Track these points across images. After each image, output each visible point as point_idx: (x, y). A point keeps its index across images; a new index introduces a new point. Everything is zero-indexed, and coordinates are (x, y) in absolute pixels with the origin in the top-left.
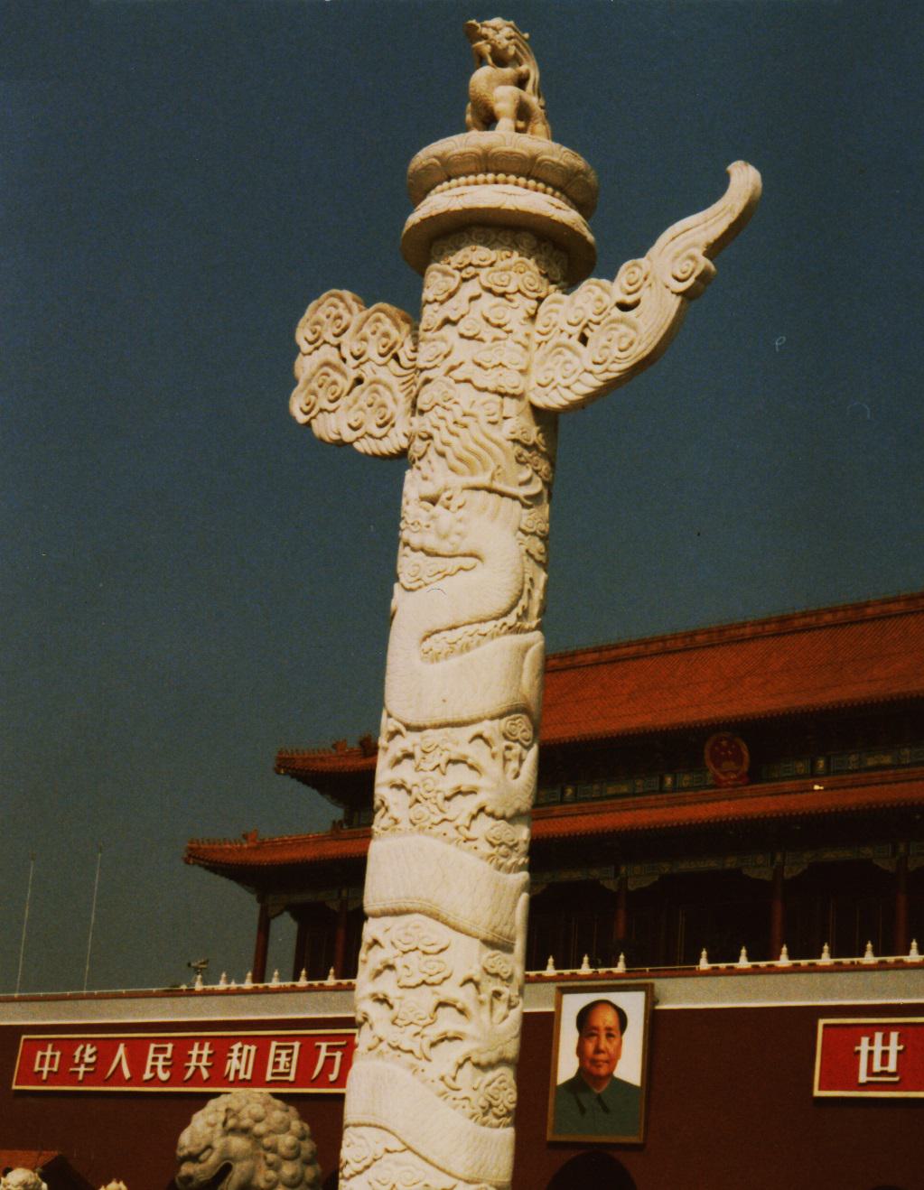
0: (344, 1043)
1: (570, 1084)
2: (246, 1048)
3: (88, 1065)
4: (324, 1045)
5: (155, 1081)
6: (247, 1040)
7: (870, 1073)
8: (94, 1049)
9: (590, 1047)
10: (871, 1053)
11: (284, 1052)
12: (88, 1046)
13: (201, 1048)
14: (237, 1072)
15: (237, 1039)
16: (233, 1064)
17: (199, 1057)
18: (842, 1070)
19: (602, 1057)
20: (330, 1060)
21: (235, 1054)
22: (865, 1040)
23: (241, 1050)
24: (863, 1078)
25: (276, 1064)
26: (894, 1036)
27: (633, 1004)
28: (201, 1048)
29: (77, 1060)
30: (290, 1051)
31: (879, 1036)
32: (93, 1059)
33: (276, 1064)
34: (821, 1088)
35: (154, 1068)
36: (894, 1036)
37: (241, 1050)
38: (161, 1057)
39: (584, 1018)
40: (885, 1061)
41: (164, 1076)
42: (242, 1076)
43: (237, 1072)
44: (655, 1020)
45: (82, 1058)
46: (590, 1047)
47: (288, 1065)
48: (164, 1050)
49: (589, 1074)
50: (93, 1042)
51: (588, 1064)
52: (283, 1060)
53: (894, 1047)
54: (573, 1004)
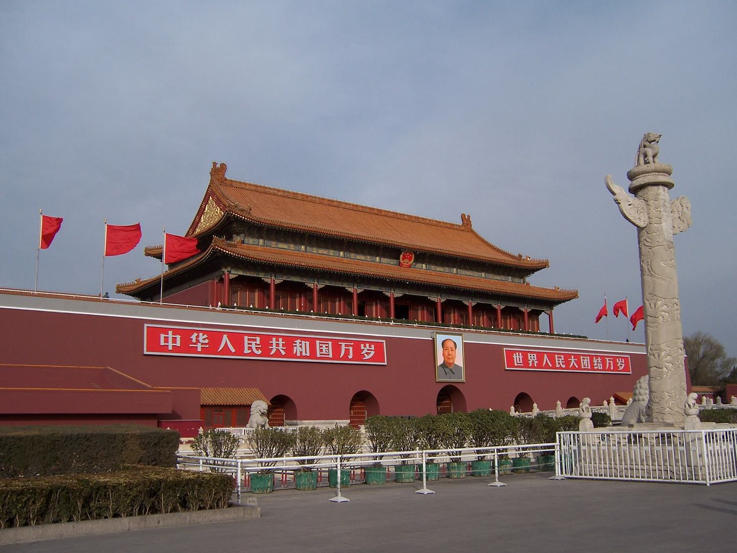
0: (353, 344)
1: (441, 365)
2: (303, 342)
3: (202, 344)
4: (343, 344)
5: (253, 354)
6: (302, 339)
7: (517, 363)
8: (206, 336)
9: (446, 354)
10: (519, 358)
11: (324, 346)
12: (201, 334)
13: (277, 340)
14: (301, 352)
15: (298, 338)
16: (297, 349)
17: (278, 345)
18: (511, 362)
19: (450, 357)
20: (347, 351)
21: (298, 345)
22: (515, 354)
23: (300, 343)
24: (516, 365)
25: (321, 350)
26: (520, 354)
27: (458, 340)
28: (277, 340)
29: (194, 341)
30: (327, 345)
31: (517, 353)
32: (207, 341)
33: (321, 350)
34: (508, 367)
35: (559, 363)
36: (520, 354)
37: (300, 343)
38: (254, 343)
39: (443, 343)
40: (520, 361)
41: (564, 366)
42: (304, 354)
43: (301, 352)
44: (466, 346)
45: (198, 341)
46: (446, 354)
47: (327, 351)
48: (561, 358)
49: (447, 362)
50: (204, 332)
51: (446, 359)
52: (324, 348)
53: (521, 357)
54: (440, 339)
